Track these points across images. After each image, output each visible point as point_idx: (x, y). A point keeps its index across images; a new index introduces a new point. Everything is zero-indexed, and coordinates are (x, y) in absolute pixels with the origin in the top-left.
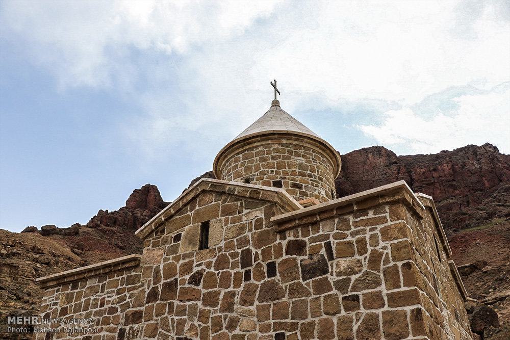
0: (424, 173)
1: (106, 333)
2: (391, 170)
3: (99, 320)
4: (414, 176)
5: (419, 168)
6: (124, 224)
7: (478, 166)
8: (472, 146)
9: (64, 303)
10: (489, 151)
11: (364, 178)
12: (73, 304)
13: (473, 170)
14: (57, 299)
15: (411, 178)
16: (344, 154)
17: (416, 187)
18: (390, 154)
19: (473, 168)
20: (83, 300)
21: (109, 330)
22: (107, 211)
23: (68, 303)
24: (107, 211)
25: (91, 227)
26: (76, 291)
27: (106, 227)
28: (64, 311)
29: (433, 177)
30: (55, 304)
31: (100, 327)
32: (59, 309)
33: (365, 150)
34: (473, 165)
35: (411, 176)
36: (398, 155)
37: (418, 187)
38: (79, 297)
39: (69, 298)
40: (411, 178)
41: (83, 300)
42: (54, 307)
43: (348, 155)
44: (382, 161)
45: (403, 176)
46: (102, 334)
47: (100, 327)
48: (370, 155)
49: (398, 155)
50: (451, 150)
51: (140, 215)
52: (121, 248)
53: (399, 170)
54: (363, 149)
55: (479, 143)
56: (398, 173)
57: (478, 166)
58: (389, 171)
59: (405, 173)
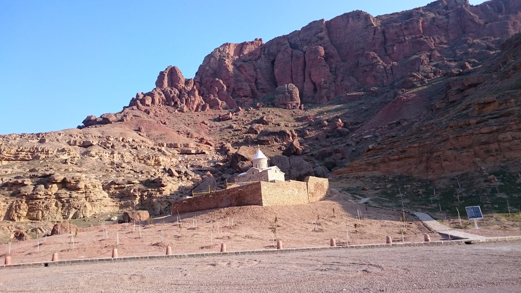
0: (396, 33)
2: (368, 32)
4: (387, 36)
5: (392, 28)
7: (445, 20)
11: (346, 41)
13: (440, 25)
15: (385, 38)
16: (329, 20)
17: (388, 47)
18: (367, 17)
19: (441, 23)
29: (404, 35)
33: (346, 16)
34: (441, 20)
35: (385, 37)
37: (391, 45)
40: (385, 38)
43: (332, 20)
44: (361, 24)
45: (378, 37)
48: (350, 19)
53: (375, 32)
54: (345, 14)
56: (374, 34)
57: (445, 20)
58: (367, 33)
59: (380, 33)
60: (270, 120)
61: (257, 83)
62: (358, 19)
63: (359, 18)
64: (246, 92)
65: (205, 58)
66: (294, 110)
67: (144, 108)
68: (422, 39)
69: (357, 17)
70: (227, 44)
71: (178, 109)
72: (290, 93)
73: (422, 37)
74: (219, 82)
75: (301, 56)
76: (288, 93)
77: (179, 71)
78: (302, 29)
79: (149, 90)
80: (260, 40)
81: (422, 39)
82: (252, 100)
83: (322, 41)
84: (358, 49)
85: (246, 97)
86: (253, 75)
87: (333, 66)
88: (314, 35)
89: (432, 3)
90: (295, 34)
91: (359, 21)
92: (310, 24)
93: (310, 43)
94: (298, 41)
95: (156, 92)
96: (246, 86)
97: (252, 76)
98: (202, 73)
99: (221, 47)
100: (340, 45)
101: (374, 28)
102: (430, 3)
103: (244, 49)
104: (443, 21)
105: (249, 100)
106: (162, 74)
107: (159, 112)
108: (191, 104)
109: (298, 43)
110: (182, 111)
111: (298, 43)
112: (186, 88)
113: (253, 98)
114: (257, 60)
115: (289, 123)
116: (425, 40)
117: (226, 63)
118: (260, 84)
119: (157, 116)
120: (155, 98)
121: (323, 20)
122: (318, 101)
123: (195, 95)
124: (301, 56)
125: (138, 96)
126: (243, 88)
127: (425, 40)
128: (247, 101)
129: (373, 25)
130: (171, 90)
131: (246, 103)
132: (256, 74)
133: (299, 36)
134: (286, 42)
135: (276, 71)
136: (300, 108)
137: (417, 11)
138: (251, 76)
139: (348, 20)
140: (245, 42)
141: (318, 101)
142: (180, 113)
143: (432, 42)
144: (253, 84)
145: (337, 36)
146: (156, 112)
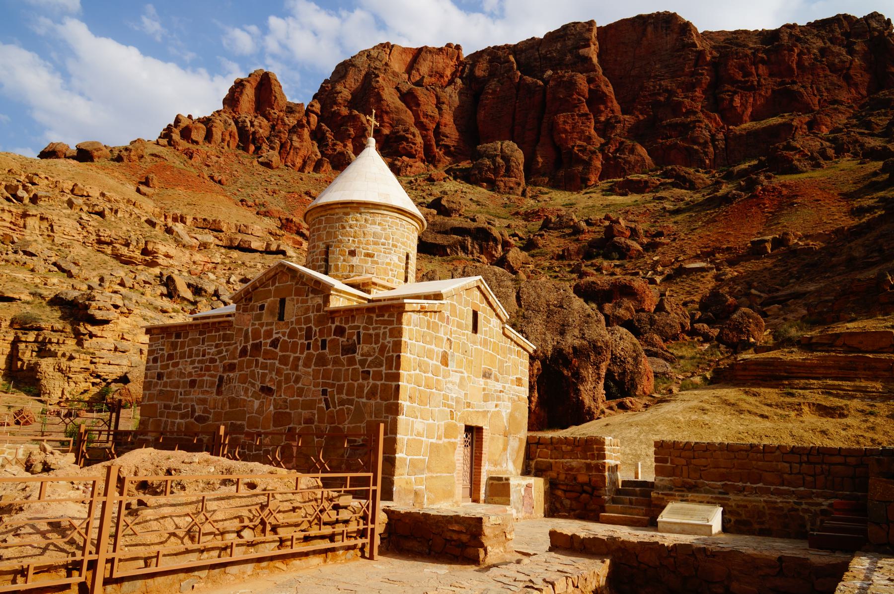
1: (209, 378)
3: (202, 367)
6: (223, 140)
8: (846, 16)
9: (170, 349)
10: (875, 29)
12: (178, 351)
14: (164, 345)
16: (604, 25)
18: (686, 28)
20: (187, 349)
21: (211, 376)
22: (190, 117)
23: (174, 350)
24: (190, 117)
25: (164, 146)
26: (179, 340)
27: (190, 146)
28: (170, 357)
30: (161, 350)
31: (203, 372)
32: (166, 354)
33: (641, 21)
34: (839, 54)
36: (700, 31)
38: (183, 345)
39: (174, 346)
41: (187, 349)
42: (161, 352)
43: (609, 26)
46: (205, 378)
47: (203, 372)
48: (650, 29)
49: (700, 31)
50: (802, 22)
51: (249, 125)
52: (220, 182)
54: (640, 17)
55: (859, 12)
60: (454, 206)
61: (440, 133)
62: (666, 30)
63: (669, 27)
64: (413, 146)
65: (337, 67)
66: (511, 196)
67: (184, 144)
68: (795, 87)
69: (664, 25)
70: (388, 43)
71: (260, 160)
72: (506, 159)
73: (794, 83)
74: (359, 118)
75: (537, 89)
76: (503, 158)
77: (276, 82)
78: (546, 36)
79: (205, 111)
80: (458, 47)
81: (795, 87)
82: (422, 164)
83: (586, 65)
84: (658, 90)
85: (411, 156)
86: (432, 114)
87: (603, 119)
88: (570, 51)
89: (816, 22)
90: (532, 44)
91: (667, 35)
92: (565, 28)
93: (558, 67)
94: (535, 59)
95: (219, 118)
96: (414, 135)
97: (431, 116)
98: (327, 96)
99: (374, 48)
100: (621, 78)
101: (697, 51)
102: (813, 22)
103: (421, 61)
104: (842, 57)
105: (417, 164)
106: (239, 85)
107: (214, 159)
108: (291, 154)
109: (535, 63)
110: (268, 165)
111: (535, 63)
112: (286, 119)
113: (426, 163)
114: (446, 87)
115: (496, 220)
116: (802, 90)
117: (378, 82)
118: (443, 136)
119: (208, 166)
120: (214, 129)
121: (591, 23)
122: (561, 184)
123: (302, 135)
124: (537, 89)
125: (178, 120)
126: (407, 138)
127: (802, 90)
128: (411, 166)
129: (696, 47)
130: (254, 119)
131: (409, 169)
132: (439, 114)
133: (538, 50)
134: (512, 58)
135: (481, 115)
136: (524, 194)
137: (789, 30)
138: (427, 115)
139: (645, 30)
140: (426, 47)
141: (561, 184)
142: (261, 168)
143: (816, 96)
144: (431, 133)
145: (616, 60)
146: (208, 157)
